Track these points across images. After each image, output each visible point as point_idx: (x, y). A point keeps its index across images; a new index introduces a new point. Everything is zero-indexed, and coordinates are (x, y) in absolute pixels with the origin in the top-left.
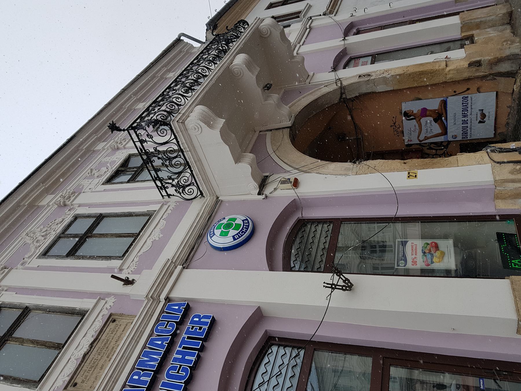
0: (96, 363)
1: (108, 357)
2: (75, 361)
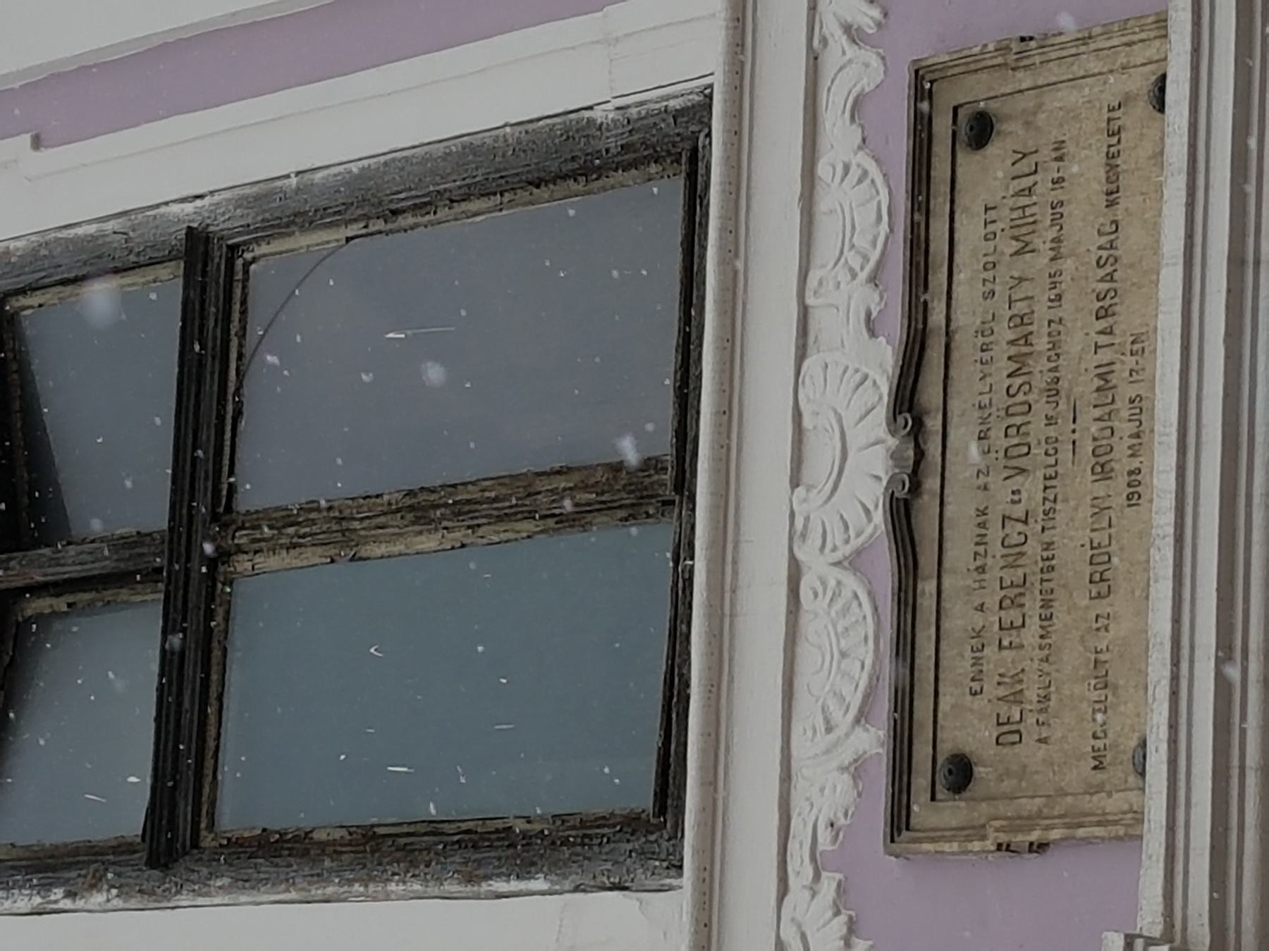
1: (1103, 471)
2: (852, 583)
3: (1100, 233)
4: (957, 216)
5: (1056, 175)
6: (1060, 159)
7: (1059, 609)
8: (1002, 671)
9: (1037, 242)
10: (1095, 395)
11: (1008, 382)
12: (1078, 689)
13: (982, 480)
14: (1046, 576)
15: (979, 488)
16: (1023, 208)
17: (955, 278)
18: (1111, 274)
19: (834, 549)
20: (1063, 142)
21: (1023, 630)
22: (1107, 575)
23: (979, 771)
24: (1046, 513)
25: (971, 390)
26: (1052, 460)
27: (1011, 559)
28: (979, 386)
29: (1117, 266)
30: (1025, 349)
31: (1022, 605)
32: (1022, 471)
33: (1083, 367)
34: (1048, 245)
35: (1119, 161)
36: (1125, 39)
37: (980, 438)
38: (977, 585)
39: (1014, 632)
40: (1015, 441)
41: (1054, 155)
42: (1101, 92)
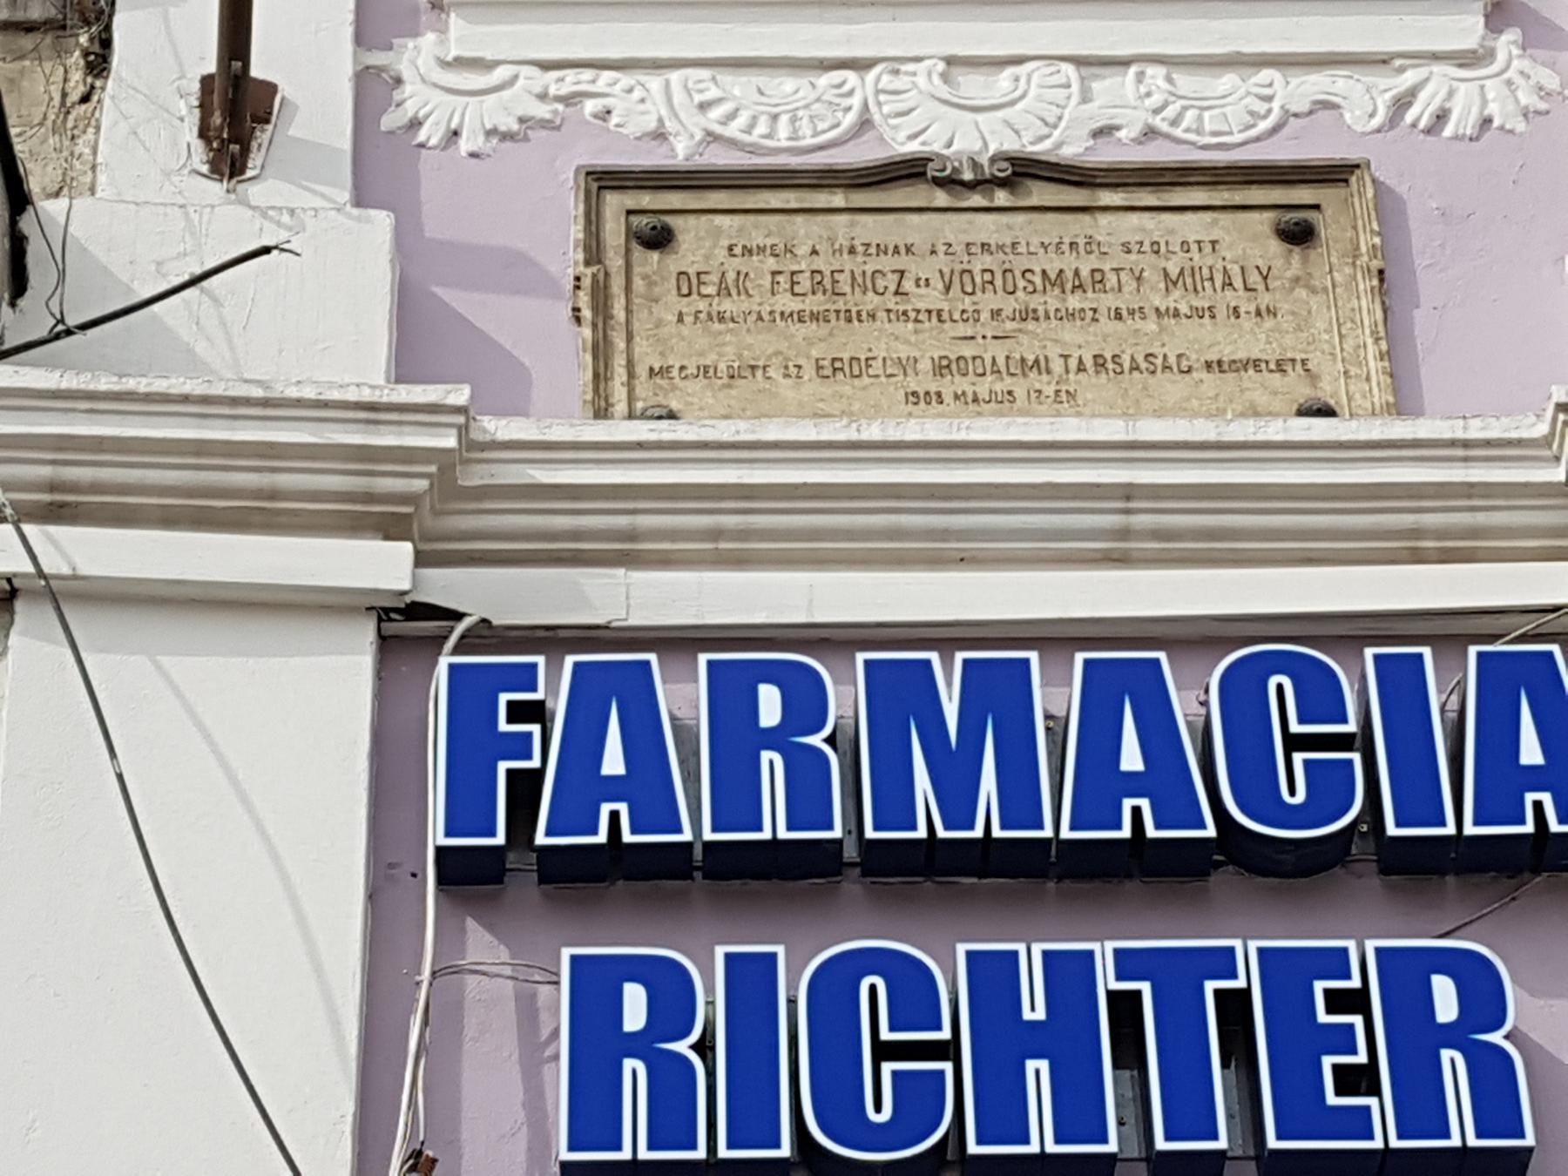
0: (872, 301)
1: (942, 368)
3: (1179, 356)
8: (752, 275)
9: (1177, 293)
10: (1018, 357)
11: (1038, 270)
13: (941, 249)
14: (842, 315)
16: (1211, 279)
17: (1147, 215)
18: (1137, 368)
20: (1275, 315)
21: (789, 295)
22: (840, 375)
24: (905, 313)
25: (1029, 233)
26: (957, 316)
27: (860, 280)
28: (1035, 241)
29: (1146, 374)
30: (1069, 286)
31: (814, 293)
32: (948, 289)
33: (1049, 344)
34: (1172, 305)
35: (1251, 372)
36: (1373, 373)
37: (983, 245)
38: (837, 246)
39: (788, 286)
40: (978, 280)
42: (1323, 352)
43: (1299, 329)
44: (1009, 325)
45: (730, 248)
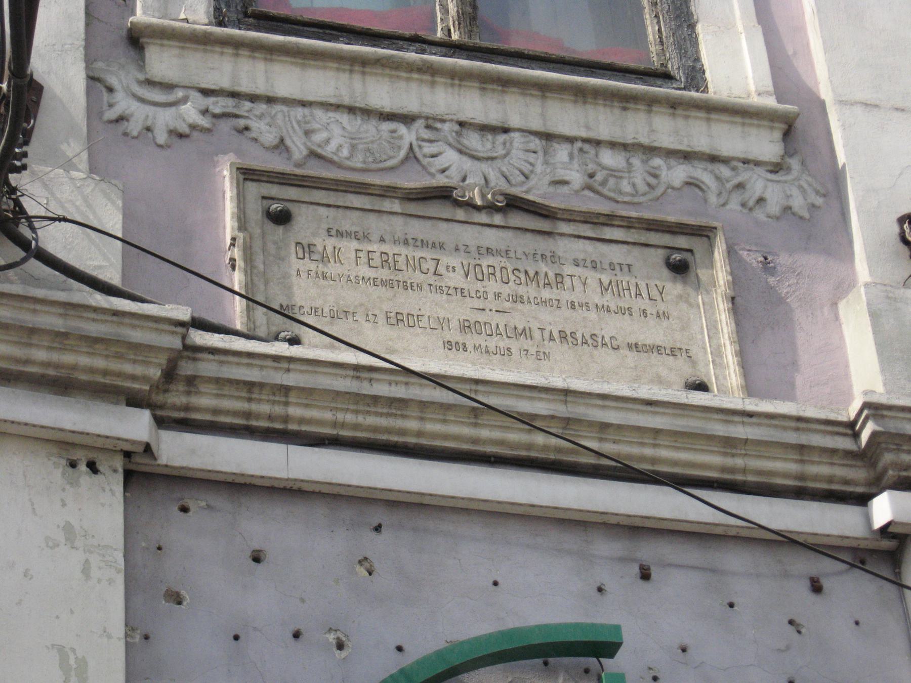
0: (418, 277)
4: (625, 246)
5: (648, 313)
6: (658, 316)
7: (381, 291)
11: (522, 270)
12: (331, 299)
13: (462, 248)
14: (401, 284)
15: (457, 246)
19: (420, 147)
23: (280, 229)
26: (473, 295)
29: (591, 347)
30: (541, 284)
33: (531, 320)
34: (606, 304)
37: (488, 249)
38: (396, 238)
39: (366, 260)
41: (661, 312)
43: (683, 329)
44: (508, 305)
45: (329, 230)
